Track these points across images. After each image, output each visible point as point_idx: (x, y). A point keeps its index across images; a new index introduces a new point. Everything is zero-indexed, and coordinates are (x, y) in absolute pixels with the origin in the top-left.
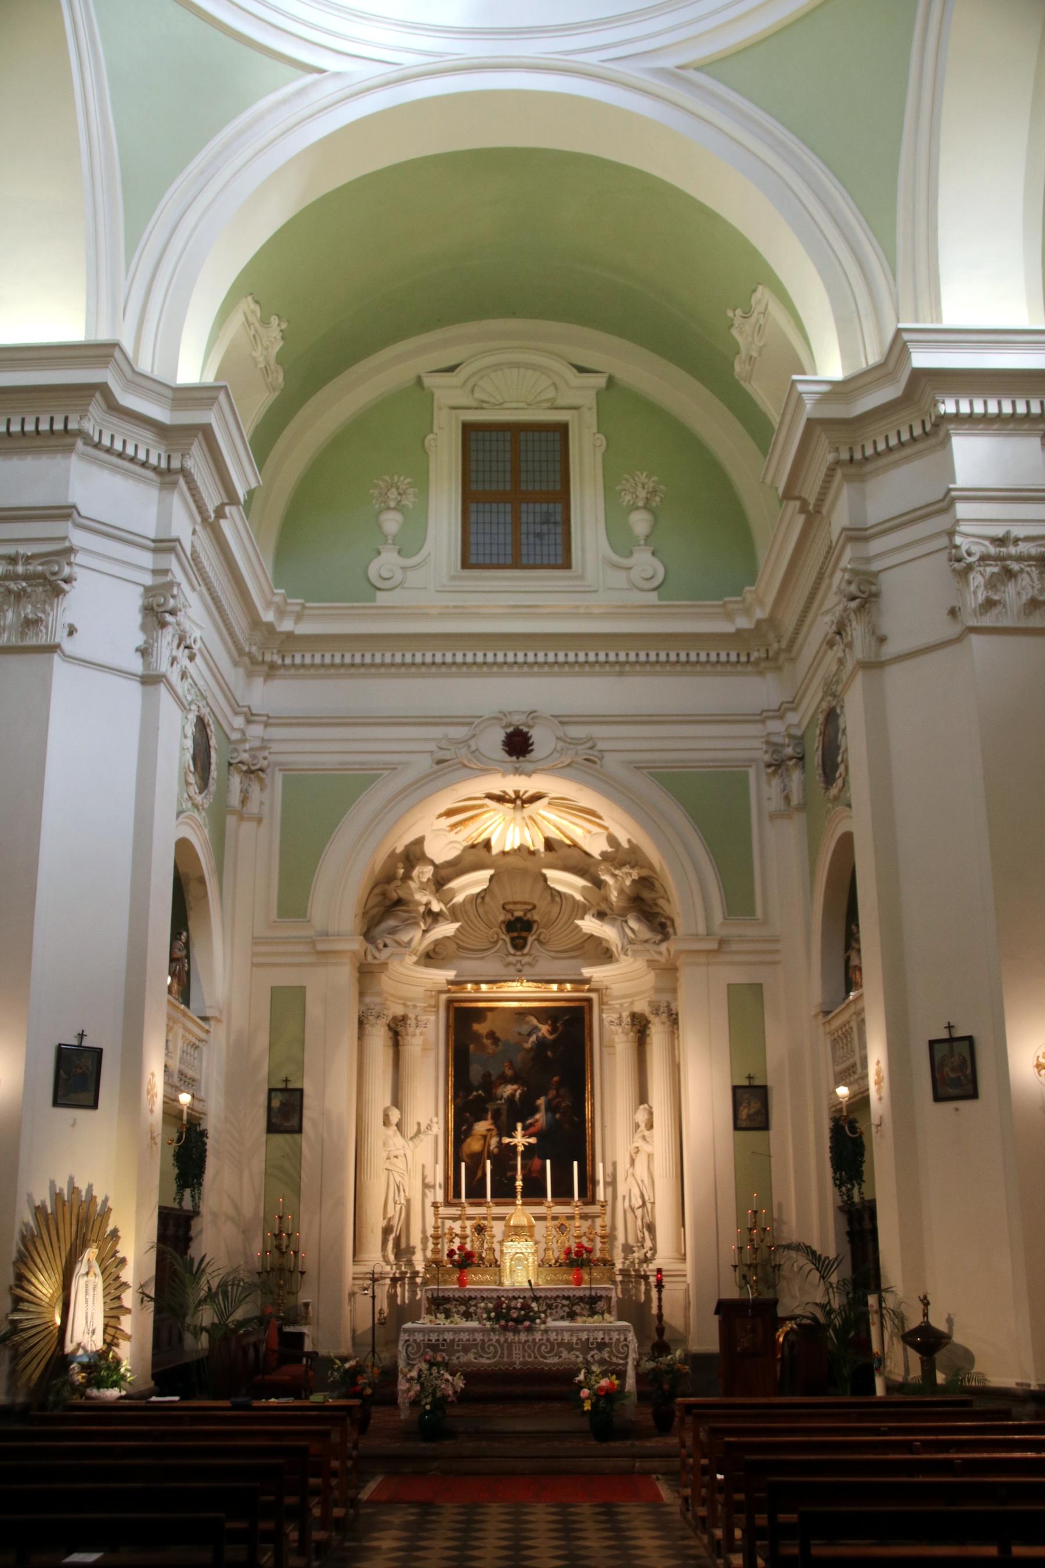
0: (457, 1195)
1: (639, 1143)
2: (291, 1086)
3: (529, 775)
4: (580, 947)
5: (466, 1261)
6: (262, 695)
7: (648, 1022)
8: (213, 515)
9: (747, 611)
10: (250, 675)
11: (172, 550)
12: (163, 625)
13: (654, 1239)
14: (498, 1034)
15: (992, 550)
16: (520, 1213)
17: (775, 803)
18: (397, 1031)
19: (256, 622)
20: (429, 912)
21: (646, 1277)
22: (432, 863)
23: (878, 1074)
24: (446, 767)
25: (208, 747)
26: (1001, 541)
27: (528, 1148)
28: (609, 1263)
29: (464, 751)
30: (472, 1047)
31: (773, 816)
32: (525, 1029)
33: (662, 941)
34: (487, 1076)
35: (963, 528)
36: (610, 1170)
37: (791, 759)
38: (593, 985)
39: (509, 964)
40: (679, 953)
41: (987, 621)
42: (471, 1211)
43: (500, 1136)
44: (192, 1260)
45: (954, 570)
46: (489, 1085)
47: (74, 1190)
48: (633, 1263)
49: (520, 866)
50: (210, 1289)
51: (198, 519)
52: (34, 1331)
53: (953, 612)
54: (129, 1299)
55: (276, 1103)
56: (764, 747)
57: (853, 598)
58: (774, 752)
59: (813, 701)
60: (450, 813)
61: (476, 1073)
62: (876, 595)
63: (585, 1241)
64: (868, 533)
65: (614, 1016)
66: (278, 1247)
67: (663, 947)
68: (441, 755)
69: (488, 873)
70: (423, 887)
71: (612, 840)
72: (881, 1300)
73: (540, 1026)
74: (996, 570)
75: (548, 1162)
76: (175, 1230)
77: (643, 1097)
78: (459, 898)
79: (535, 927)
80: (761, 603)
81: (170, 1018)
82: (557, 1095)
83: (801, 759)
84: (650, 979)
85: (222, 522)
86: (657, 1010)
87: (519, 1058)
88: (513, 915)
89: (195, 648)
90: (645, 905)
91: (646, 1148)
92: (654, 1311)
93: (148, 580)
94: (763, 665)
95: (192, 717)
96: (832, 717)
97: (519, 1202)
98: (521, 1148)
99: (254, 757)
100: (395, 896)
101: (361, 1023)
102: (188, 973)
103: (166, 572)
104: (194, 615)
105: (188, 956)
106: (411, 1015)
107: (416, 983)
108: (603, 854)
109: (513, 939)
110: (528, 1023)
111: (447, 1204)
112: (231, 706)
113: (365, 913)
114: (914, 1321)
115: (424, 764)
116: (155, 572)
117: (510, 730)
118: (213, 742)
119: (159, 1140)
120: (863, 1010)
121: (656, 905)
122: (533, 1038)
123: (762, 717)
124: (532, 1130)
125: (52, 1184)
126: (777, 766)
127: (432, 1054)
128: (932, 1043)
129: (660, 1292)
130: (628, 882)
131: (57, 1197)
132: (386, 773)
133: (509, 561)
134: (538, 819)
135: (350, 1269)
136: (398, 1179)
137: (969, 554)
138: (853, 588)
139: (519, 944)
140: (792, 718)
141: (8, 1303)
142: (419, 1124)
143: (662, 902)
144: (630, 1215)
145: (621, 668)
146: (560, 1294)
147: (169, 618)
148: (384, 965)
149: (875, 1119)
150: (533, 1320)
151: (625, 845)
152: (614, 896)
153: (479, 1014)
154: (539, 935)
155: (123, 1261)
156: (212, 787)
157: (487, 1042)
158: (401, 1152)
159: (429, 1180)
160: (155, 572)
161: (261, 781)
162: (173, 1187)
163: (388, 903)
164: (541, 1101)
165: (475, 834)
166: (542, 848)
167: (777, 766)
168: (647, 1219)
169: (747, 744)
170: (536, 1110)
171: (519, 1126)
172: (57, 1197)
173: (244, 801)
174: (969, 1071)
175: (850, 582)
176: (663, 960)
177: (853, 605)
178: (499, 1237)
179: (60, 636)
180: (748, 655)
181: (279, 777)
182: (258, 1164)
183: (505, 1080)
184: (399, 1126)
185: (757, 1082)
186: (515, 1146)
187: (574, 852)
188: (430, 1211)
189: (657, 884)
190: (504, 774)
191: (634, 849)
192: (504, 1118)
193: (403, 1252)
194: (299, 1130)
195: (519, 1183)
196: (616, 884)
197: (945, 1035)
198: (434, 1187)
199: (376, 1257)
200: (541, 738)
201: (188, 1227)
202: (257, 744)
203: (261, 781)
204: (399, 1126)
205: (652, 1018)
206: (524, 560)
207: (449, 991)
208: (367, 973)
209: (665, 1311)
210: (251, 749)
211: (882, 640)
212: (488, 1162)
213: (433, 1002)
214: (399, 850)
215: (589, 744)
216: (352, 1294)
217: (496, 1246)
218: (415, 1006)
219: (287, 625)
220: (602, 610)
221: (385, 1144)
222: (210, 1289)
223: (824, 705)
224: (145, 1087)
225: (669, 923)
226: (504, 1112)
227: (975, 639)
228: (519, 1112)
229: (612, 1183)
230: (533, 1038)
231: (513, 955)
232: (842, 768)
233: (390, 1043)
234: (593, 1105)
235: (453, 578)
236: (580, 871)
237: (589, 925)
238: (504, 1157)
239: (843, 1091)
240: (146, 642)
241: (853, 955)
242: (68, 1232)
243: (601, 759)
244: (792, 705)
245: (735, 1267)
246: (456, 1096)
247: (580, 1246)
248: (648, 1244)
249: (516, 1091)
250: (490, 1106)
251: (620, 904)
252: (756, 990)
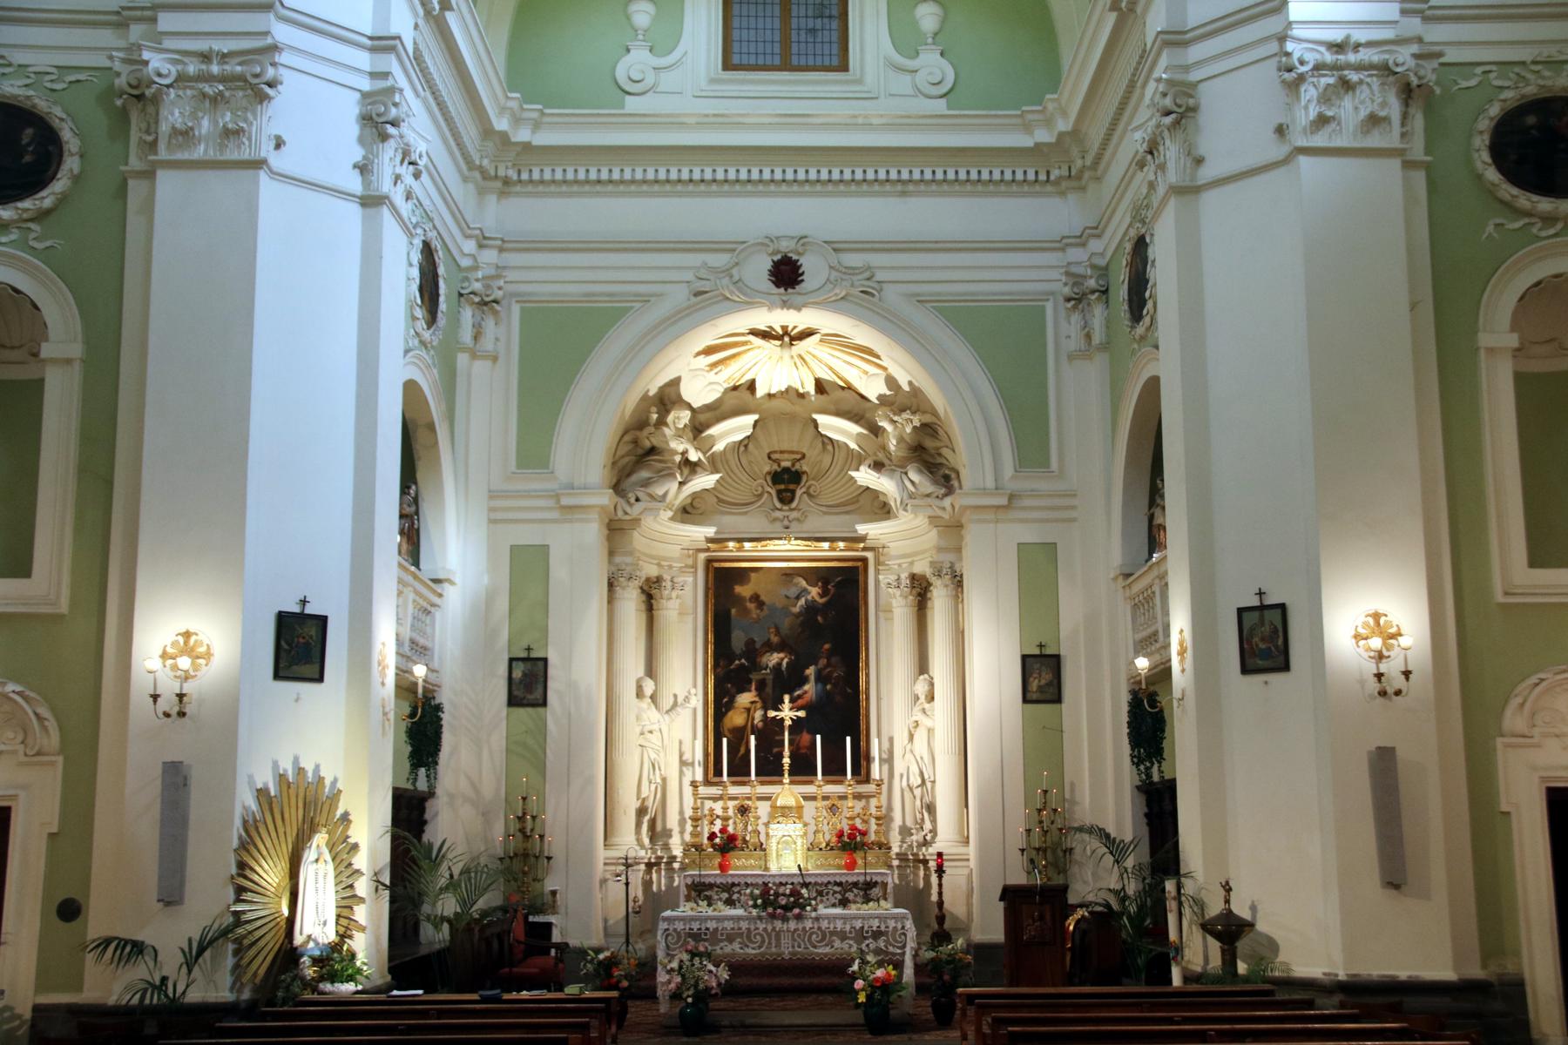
0: (718, 773)
1: (919, 717)
2: (534, 655)
3: (799, 309)
4: (855, 501)
5: (728, 844)
6: (496, 214)
7: (930, 584)
8: (437, 7)
9: (1048, 123)
10: (482, 192)
11: (392, 49)
12: (384, 137)
13: (934, 821)
14: (763, 598)
15: (1329, 57)
16: (787, 792)
17: (1075, 343)
18: (650, 595)
19: (487, 131)
20: (687, 462)
21: (925, 862)
22: (689, 406)
23: (1181, 644)
24: (706, 299)
25: (436, 276)
26: (1338, 47)
27: (797, 722)
28: (884, 846)
29: (726, 281)
30: (733, 611)
31: (1071, 357)
32: (793, 592)
33: (946, 495)
34: (750, 643)
35: (1297, 32)
36: (886, 745)
37: (1093, 292)
38: (869, 543)
39: (775, 520)
40: (965, 508)
41: (1319, 140)
42: (734, 790)
43: (765, 709)
44: (431, 845)
45: (1283, 82)
46: (753, 653)
47: (300, 771)
48: (911, 846)
49: (787, 410)
50: (452, 876)
51: (421, 12)
52: (259, 923)
53: (1280, 130)
54: (362, 887)
55: (518, 674)
56: (1064, 278)
57: (1168, 113)
58: (1075, 284)
59: (1119, 231)
60: (709, 351)
61: (738, 640)
62: (1194, 109)
63: (858, 823)
64: (1188, 36)
65: (892, 578)
66: (522, 830)
67: (947, 502)
68: (701, 285)
69: (750, 419)
70: (679, 434)
71: (891, 382)
72: (1179, 887)
74: (1331, 81)
75: (818, 737)
76: (409, 812)
77: (923, 666)
78: (719, 447)
79: (804, 478)
80: (1064, 113)
81: (400, 581)
82: (828, 665)
83: (1106, 292)
84: (932, 537)
85: (449, 16)
87: (786, 624)
89: (422, 163)
90: (928, 455)
91: (925, 722)
92: (934, 898)
93: (366, 85)
94: (1064, 184)
95: (418, 242)
96: (1141, 245)
97: (786, 779)
98: (788, 723)
99: (488, 287)
100: (647, 444)
101: (611, 585)
102: (418, 530)
103: (385, 75)
104: (419, 128)
105: (417, 513)
106: (667, 577)
107: (672, 541)
108: (881, 397)
109: (779, 492)
111: (707, 782)
112: (461, 230)
113: (614, 463)
114: (1215, 908)
115: (679, 296)
116: (374, 75)
117: (777, 257)
118: (441, 270)
119: (392, 716)
120: (1166, 573)
121: (940, 455)
122: (802, 602)
123: (1062, 245)
124: (800, 702)
125: (275, 765)
126: (1078, 300)
127: (690, 619)
128: (1241, 611)
129: (940, 877)
130: (908, 430)
131: (281, 778)
132: (637, 305)
133: (777, 61)
134: (808, 358)
135: (601, 854)
136: (653, 756)
137: (1302, 63)
138: (1168, 102)
139: (786, 498)
140: (1095, 245)
141: (231, 894)
142: (675, 696)
143: (945, 451)
144: (908, 795)
145: (903, 187)
146: (832, 879)
147: (391, 130)
148: (636, 521)
149: (1177, 693)
150: (803, 907)
151: (906, 388)
152: (892, 444)
153: (742, 575)
155: (355, 847)
156: (442, 320)
157: (751, 606)
158: (655, 727)
159: (687, 756)
160: (374, 75)
161: (496, 313)
162: (407, 765)
163: (640, 452)
164: (811, 671)
165: (737, 376)
166: (812, 392)
167: (1078, 300)
168: (927, 800)
169: (1042, 276)
170: (805, 680)
171: (787, 698)
172: (281, 778)
173: (476, 338)
174: (1280, 642)
175: (1165, 95)
176: (946, 516)
177: (1168, 120)
178: (764, 819)
179: (267, 150)
180: (1048, 173)
181: (516, 309)
182: (498, 740)
183: (770, 647)
184: (653, 698)
185: (1048, 651)
186: (782, 720)
187: (847, 394)
188: (688, 790)
189: (941, 432)
190: (770, 309)
191: (916, 391)
192: (769, 690)
193: (658, 834)
194: (544, 704)
195: (786, 761)
196: (896, 431)
197: (1255, 602)
198: (692, 764)
199: (629, 841)
200: (810, 265)
201: (422, 810)
202: (493, 272)
203: (496, 313)
204: (653, 698)
205: (933, 580)
206: (795, 61)
207: (708, 550)
208: (616, 531)
209: (945, 898)
210: (484, 278)
211: (1199, 161)
212: (753, 738)
213: (690, 562)
214: (651, 393)
215: (867, 274)
216: (604, 881)
217: (761, 828)
218: (670, 567)
219: (523, 135)
220: (883, 121)
221: (638, 718)
222: (452, 876)
223: (1133, 233)
224: (376, 657)
225: (953, 475)
227: (1303, 161)
228: (787, 682)
229: (889, 760)
230: (802, 602)
232: (1150, 305)
233: (643, 607)
234: (867, 675)
235: (713, 81)
236: (856, 418)
237: (865, 476)
238: (770, 733)
239: (1142, 663)
240: (365, 158)
241: (1157, 512)
242: (294, 816)
243: (880, 291)
244: (1096, 231)
245: (1023, 850)
246: (716, 665)
247: (853, 828)
248: (928, 825)
250: (755, 677)
251: (900, 454)
252: (1050, 549)
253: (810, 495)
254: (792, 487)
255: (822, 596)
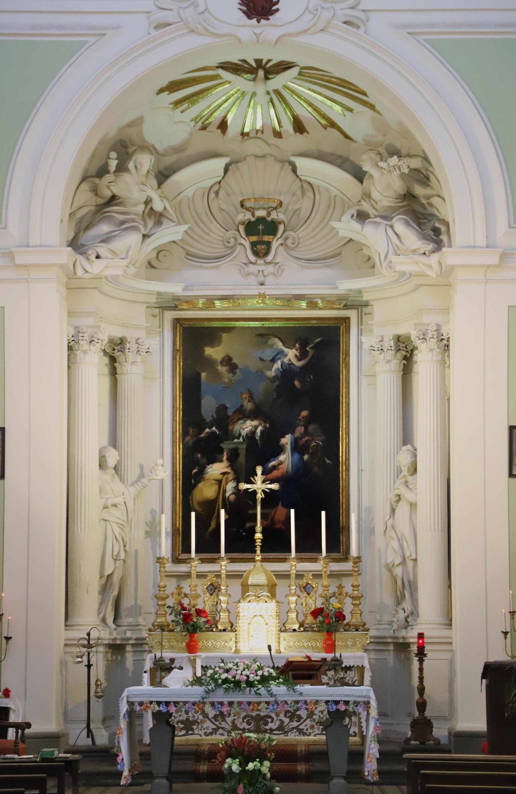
14: (235, 361)
30: (203, 375)
32: (268, 354)
46: (223, 419)
61: (208, 406)
73: (286, 350)
79: (281, 228)
87: (260, 389)
88: (253, 215)
98: (260, 496)
109: (253, 245)
110: (272, 346)
122: (278, 365)
139: (260, 250)
142: (141, 467)
154: (286, 239)
157: (223, 369)
226: (242, 452)
230: (278, 365)
246: (185, 433)
249: (256, 427)
250: (226, 446)
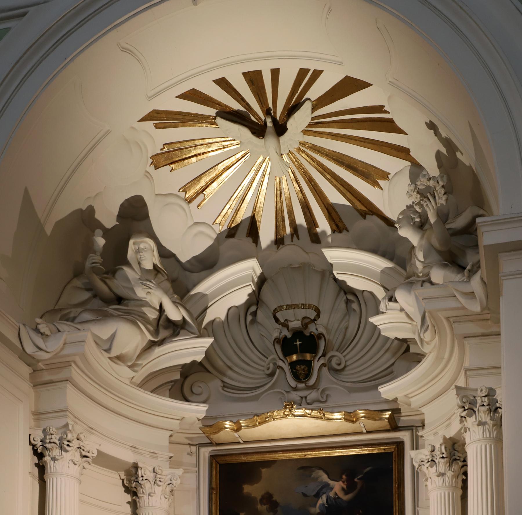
32: (312, 489)
86: (473, 403)
109: (293, 365)
110: (316, 479)
122: (323, 500)
230: (323, 500)
231: (295, 389)
253: (331, 369)
254: (308, 357)
255: (346, 492)
